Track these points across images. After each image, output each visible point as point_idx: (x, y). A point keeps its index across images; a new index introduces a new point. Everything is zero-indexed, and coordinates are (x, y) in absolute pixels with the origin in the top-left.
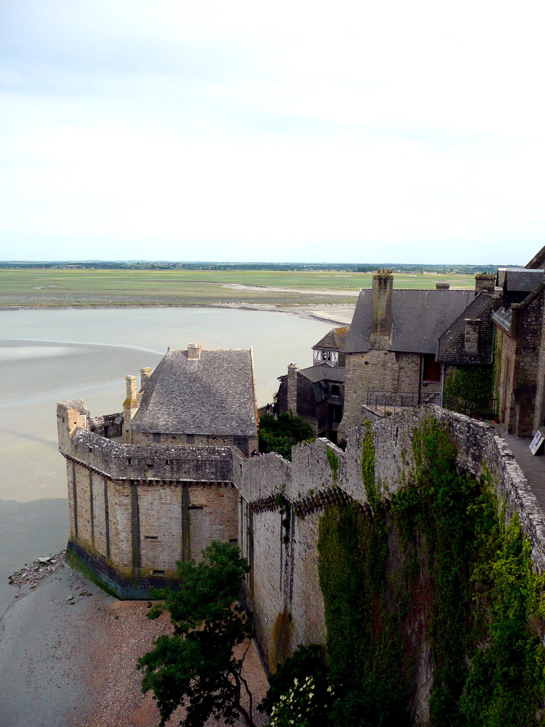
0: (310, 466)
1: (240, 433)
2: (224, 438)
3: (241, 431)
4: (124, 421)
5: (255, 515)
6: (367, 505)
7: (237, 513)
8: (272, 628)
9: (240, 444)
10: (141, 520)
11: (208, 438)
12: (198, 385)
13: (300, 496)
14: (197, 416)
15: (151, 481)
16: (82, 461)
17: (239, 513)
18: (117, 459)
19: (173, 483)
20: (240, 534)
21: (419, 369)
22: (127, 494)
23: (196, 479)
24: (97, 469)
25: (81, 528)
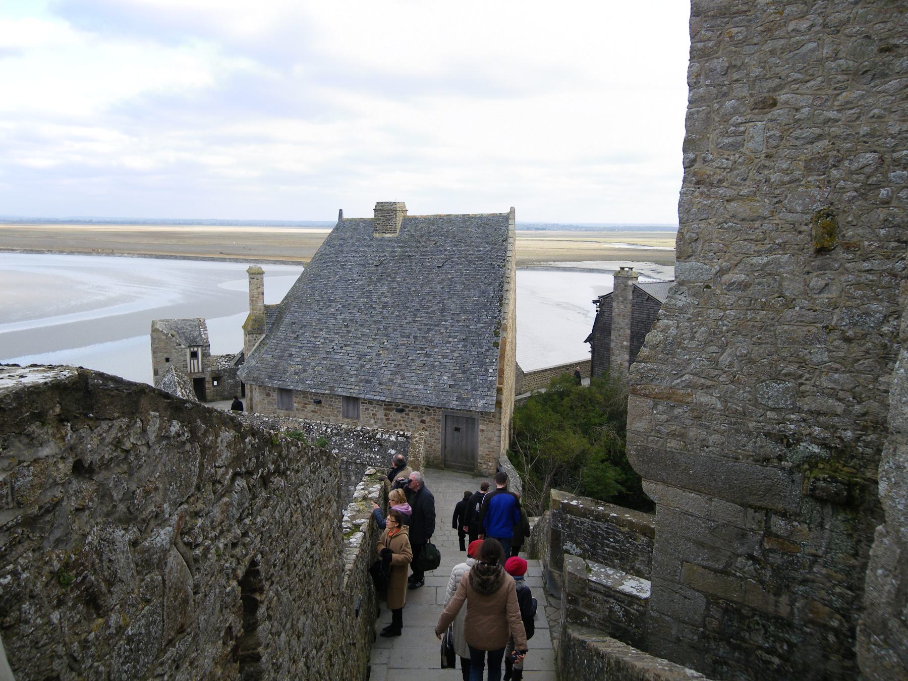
1: (454, 404)
2: (422, 412)
9: (457, 430)
12: (385, 289)
14: (369, 357)
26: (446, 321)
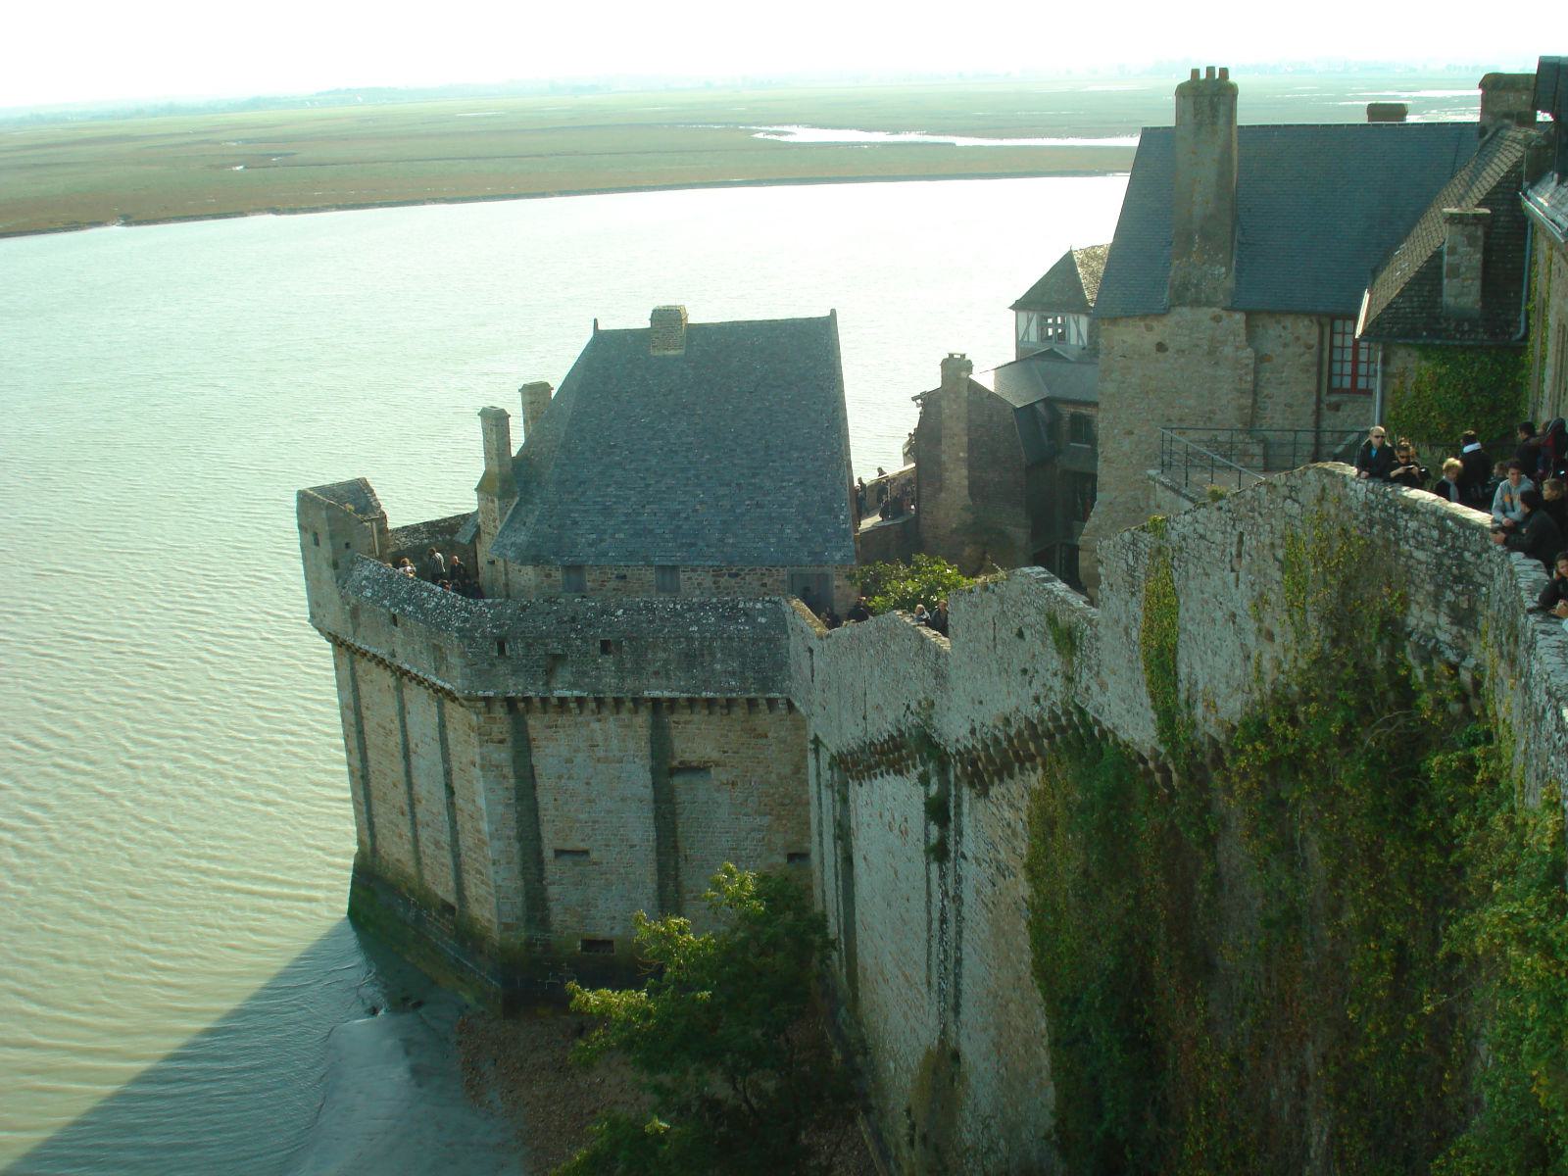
0: (999, 647)
3: (810, 553)
4: (482, 534)
5: (853, 786)
6: (1156, 754)
7: (806, 782)
8: (909, 1086)
10: (541, 805)
11: (718, 576)
13: (973, 732)
15: (563, 701)
16: (373, 650)
17: (812, 781)
18: (466, 641)
19: (624, 702)
20: (816, 839)
21: (1315, 359)
22: (501, 737)
23: (688, 691)
24: (414, 671)
25: (384, 831)
26: (773, 461)
